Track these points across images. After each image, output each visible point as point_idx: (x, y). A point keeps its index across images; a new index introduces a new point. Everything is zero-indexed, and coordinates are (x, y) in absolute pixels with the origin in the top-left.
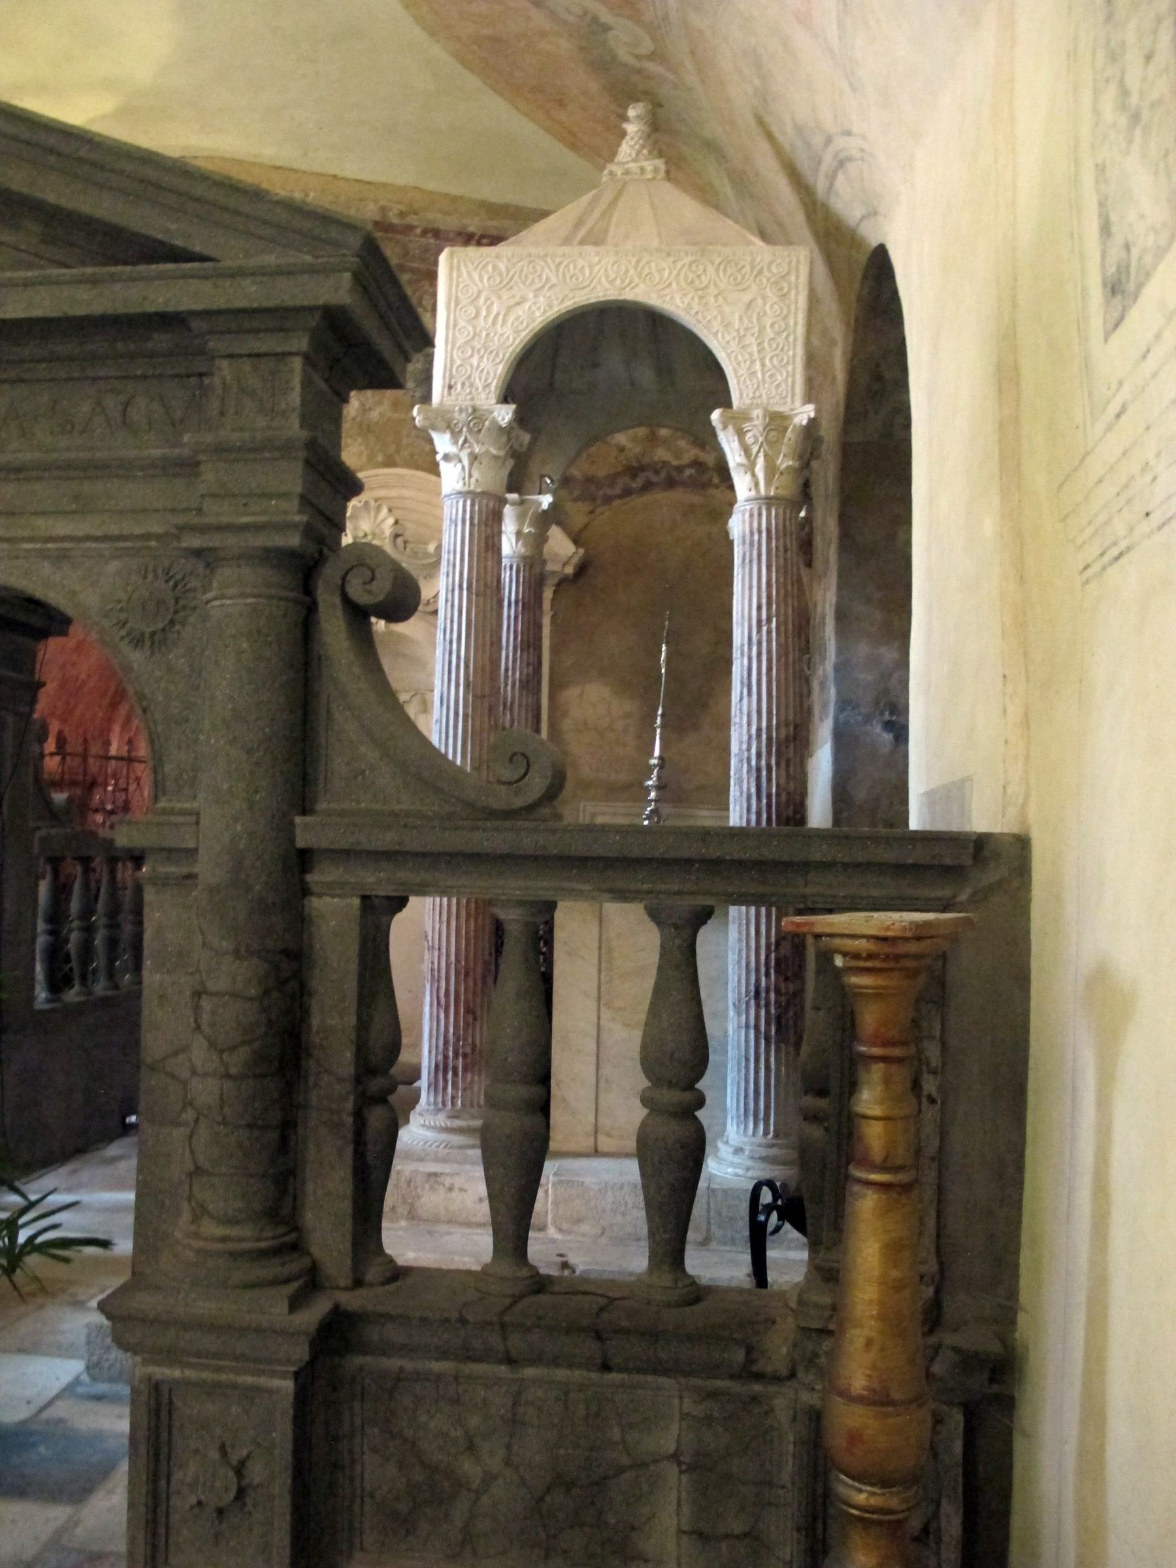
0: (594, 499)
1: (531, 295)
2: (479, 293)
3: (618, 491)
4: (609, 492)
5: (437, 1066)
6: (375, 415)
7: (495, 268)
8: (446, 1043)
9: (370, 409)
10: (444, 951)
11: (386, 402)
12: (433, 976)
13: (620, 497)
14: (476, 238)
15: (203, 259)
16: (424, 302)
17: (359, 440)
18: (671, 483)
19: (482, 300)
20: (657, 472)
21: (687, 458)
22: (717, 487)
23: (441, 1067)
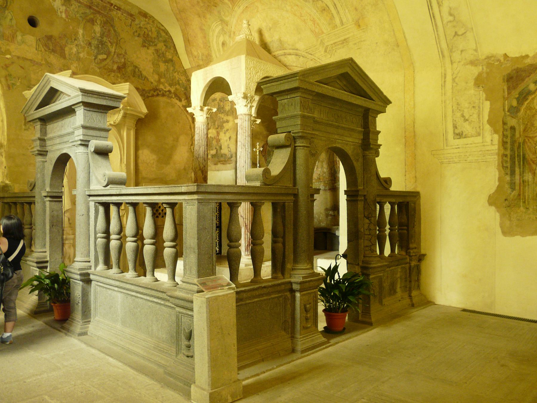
0: (145, 96)
1: (260, 71)
2: (251, 67)
3: (150, 95)
4: (148, 95)
5: (248, 245)
6: (81, 55)
7: (254, 62)
8: (249, 239)
9: (80, 53)
10: (248, 219)
11: (85, 52)
12: (246, 225)
13: (151, 97)
14: (114, 5)
15: (374, 101)
16: (97, 21)
17: (77, 62)
18: (163, 95)
19: (252, 69)
20: (160, 91)
21: (167, 89)
22: (173, 98)
23: (249, 245)
